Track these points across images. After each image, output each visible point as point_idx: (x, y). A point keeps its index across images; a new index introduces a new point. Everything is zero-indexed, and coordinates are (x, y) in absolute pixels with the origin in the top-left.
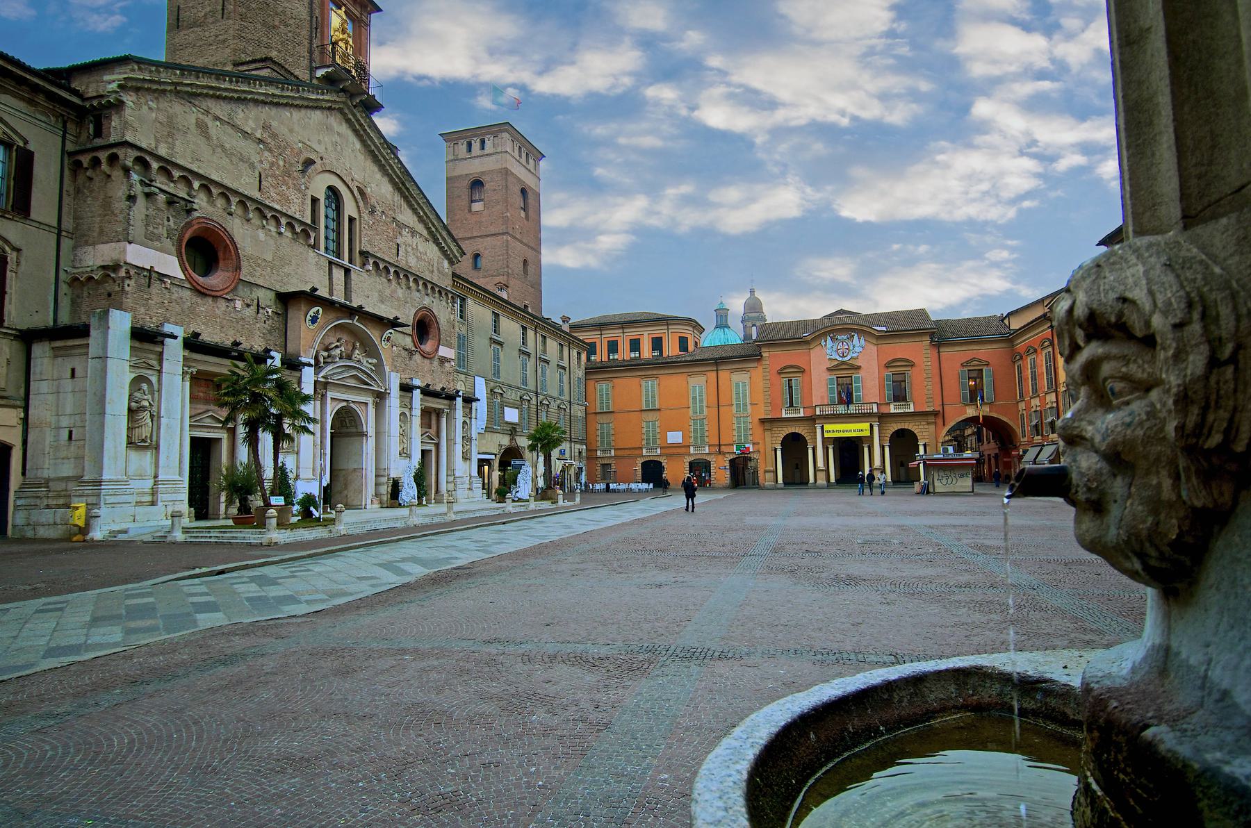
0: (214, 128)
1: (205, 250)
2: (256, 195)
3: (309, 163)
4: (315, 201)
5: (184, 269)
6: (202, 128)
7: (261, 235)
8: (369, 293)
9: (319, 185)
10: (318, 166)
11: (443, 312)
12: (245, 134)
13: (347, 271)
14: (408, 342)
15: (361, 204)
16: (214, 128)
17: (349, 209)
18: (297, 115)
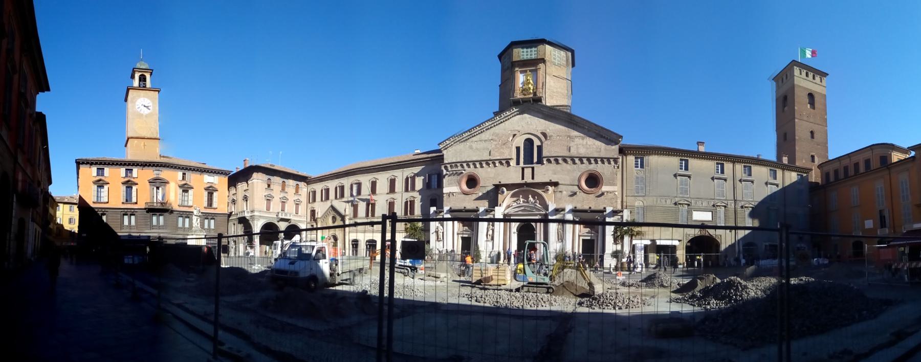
0: (474, 145)
1: (472, 182)
2: (488, 158)
3: (514, 135)
4: (518, 149)
5: (461, 188)
6: (471, 147)
7: (489, 169)
8: (543, 173)
9: (520, 142)
10: (518, 134)
11: (603, 169)
12: (485, 141)
13: (533, 168)
14: (576, 189)
15: (543, 138)
16: (474, 145)
17: (537, 143)
18: (507, 123)
